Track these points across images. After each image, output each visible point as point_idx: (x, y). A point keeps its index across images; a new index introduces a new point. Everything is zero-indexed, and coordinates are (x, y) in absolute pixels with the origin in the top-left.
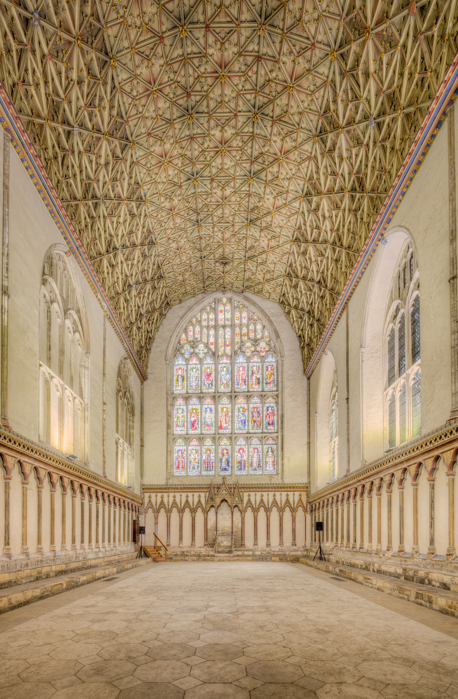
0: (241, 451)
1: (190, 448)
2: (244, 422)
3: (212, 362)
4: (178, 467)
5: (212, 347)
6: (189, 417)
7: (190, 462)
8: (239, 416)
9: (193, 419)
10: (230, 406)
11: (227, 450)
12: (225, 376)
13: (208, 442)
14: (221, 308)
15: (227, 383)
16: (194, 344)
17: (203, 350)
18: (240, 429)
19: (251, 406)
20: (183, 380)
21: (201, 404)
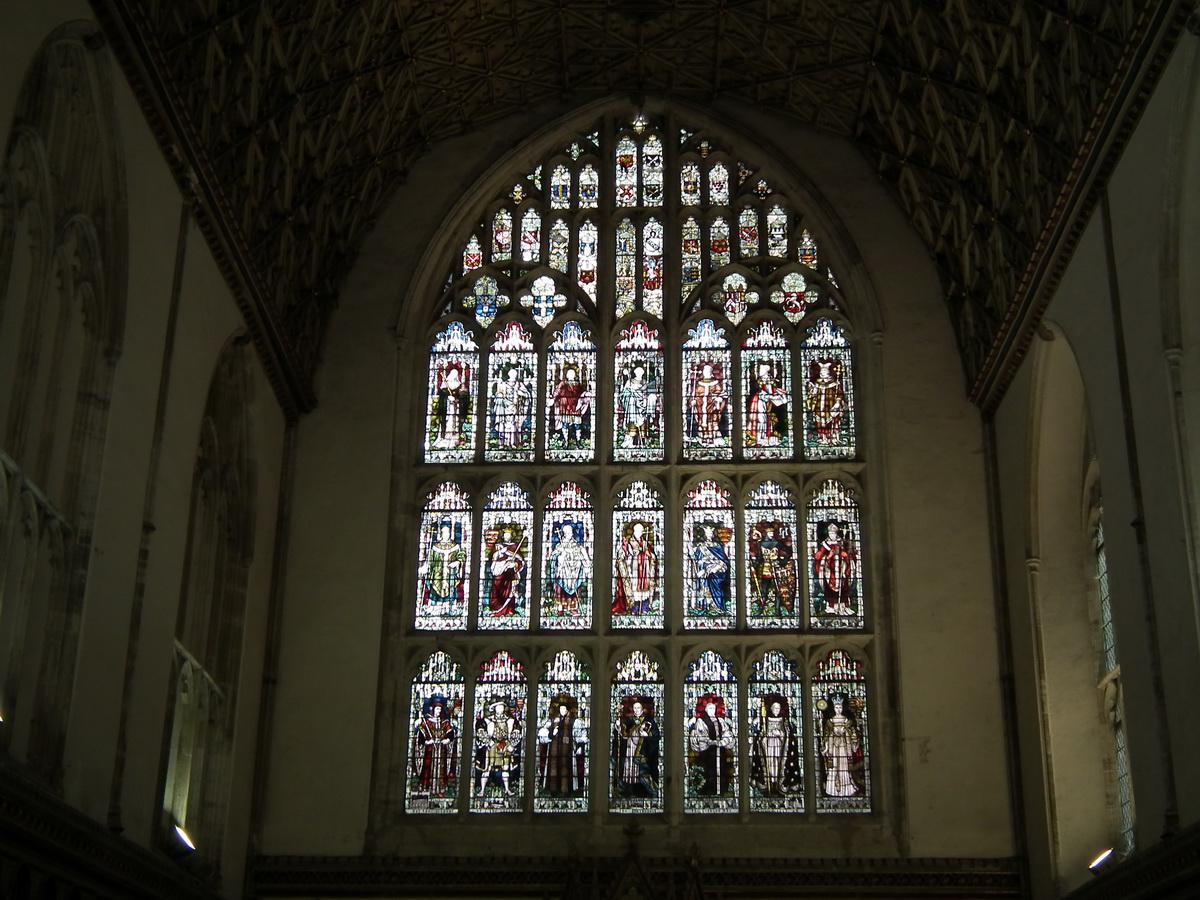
0: (711, 709)
1: (481, 690)
2: (719, 584)
3: (587, 345)
4: (424, 779)
5: (590, 289)
6: (484, 558)
7: (481, 754)
8: (700, 561)
9: (498, 569)
10: (660, 515)
11: (647, 702)
12: (638, 399)
13: (564, 668)
14: (626, 149)
15: (647, 424)
16: (515, 277)
17: (549, 299)
18: (704, 610)
19: (752, 517)
20: (464, 414)
21: (539, 505)
